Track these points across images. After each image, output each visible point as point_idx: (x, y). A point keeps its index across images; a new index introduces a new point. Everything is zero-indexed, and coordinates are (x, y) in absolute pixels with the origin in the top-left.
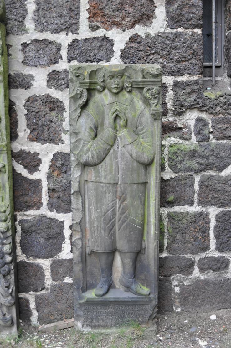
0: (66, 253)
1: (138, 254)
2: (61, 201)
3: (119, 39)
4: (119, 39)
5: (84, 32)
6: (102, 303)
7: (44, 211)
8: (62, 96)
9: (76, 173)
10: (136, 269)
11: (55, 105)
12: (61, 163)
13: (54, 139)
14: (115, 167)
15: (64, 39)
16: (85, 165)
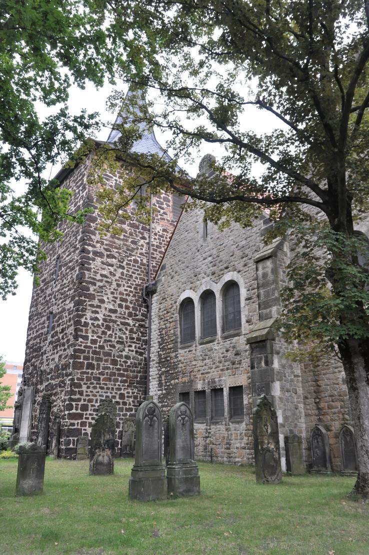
0: (119, 447)
1: (131, 445)
2: (120, 438)
3: (128, 414)
4: (128, 414)
5: (124, 412)
6: (126, 454)
7: (117, 439)
8: (121, 422)
9: (124, 433)
10: (131, 449)
11: (120, 423)
12: (121, 432)
13: (119, 428)
14: (129, 432)
15: (122, 413)
16: (125, 432)
